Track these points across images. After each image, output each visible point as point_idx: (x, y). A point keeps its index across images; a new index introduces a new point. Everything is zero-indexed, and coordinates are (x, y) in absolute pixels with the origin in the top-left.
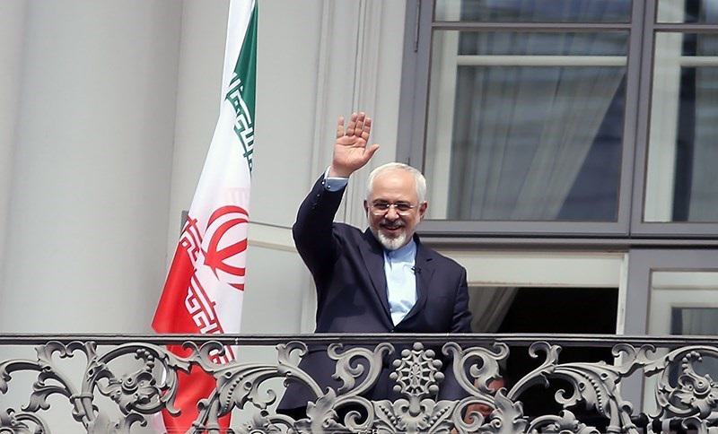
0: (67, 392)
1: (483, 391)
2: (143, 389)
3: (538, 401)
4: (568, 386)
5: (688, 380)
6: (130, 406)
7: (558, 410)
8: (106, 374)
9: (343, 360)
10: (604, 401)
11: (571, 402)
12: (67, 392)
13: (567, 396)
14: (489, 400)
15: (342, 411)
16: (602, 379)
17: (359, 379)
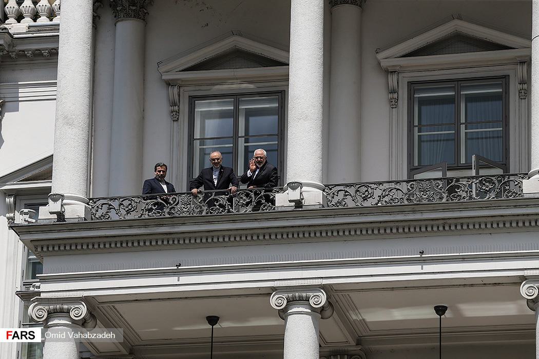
0: (114, 209)
1: (199, 203)
2: (130, 207)
3: (211, 204)
4: (217, 200)
5: (242, 198)
6: (128, 210)
7: (215, 205)
8: (122, 204)
9: (171, 198)
10: (225, 203)
11: (218, 204)
12: (114, 209)
13: (217, 203)
14: (201, 205)
15: (171, 209)
16: (224, 199)
17: (174, 203)
